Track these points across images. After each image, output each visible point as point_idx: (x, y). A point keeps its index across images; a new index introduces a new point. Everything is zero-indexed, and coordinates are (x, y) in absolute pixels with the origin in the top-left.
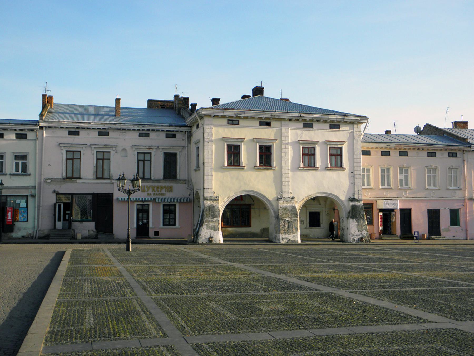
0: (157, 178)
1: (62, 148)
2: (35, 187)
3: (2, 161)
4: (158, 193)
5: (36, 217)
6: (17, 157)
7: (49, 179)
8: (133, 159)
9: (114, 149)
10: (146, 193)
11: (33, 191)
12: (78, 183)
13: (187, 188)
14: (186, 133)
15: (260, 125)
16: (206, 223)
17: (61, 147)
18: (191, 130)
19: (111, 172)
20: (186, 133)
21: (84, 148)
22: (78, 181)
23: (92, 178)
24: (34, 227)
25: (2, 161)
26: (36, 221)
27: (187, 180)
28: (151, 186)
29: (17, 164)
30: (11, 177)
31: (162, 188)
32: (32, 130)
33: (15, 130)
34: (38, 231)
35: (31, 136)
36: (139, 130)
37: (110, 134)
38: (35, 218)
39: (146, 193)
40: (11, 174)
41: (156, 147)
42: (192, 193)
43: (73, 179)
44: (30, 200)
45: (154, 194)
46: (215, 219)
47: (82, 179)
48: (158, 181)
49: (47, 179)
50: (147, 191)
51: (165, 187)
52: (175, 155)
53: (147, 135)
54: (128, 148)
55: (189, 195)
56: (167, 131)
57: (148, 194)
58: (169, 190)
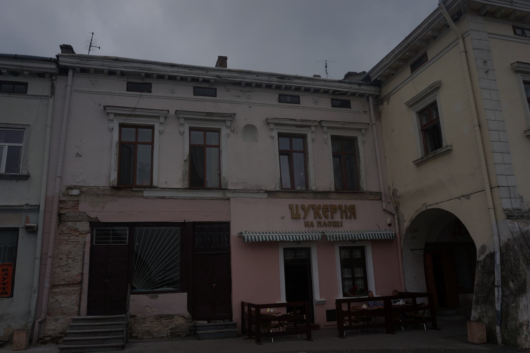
0: (321, 189)
1: (111, 117)
4: (327, 221)
5: (36, 285)
7: (75, 187)
9: (228, 123)
10: (302, 222)
11: (32, 217)
12: (147, 198)
13: (384, 210)
14: (371, 99)
17: (108, 114)
18: (380, 92)
19: (224, 174)
20: (371, 99)
21: (162, 120)
24: (29, 313)
27: (383, 193)
28: (313, 207)
31: (334, 209)
34: (37, 324)
36: (278, 87)
39: (302, 222)
41: (316, 124)
42: (396, 221)
43: (134, 189)
45: (319, 224)
47: (156, 187)
48: (325, 194)
49: (70, 188)
50: (304, 218)
51: (340, 207)
52: (353, 141)
53: (296, 100)
54: (259, 123)
55: (390, 225)
56: (334, 92)
57: (307, 225)
58: (349, 214)
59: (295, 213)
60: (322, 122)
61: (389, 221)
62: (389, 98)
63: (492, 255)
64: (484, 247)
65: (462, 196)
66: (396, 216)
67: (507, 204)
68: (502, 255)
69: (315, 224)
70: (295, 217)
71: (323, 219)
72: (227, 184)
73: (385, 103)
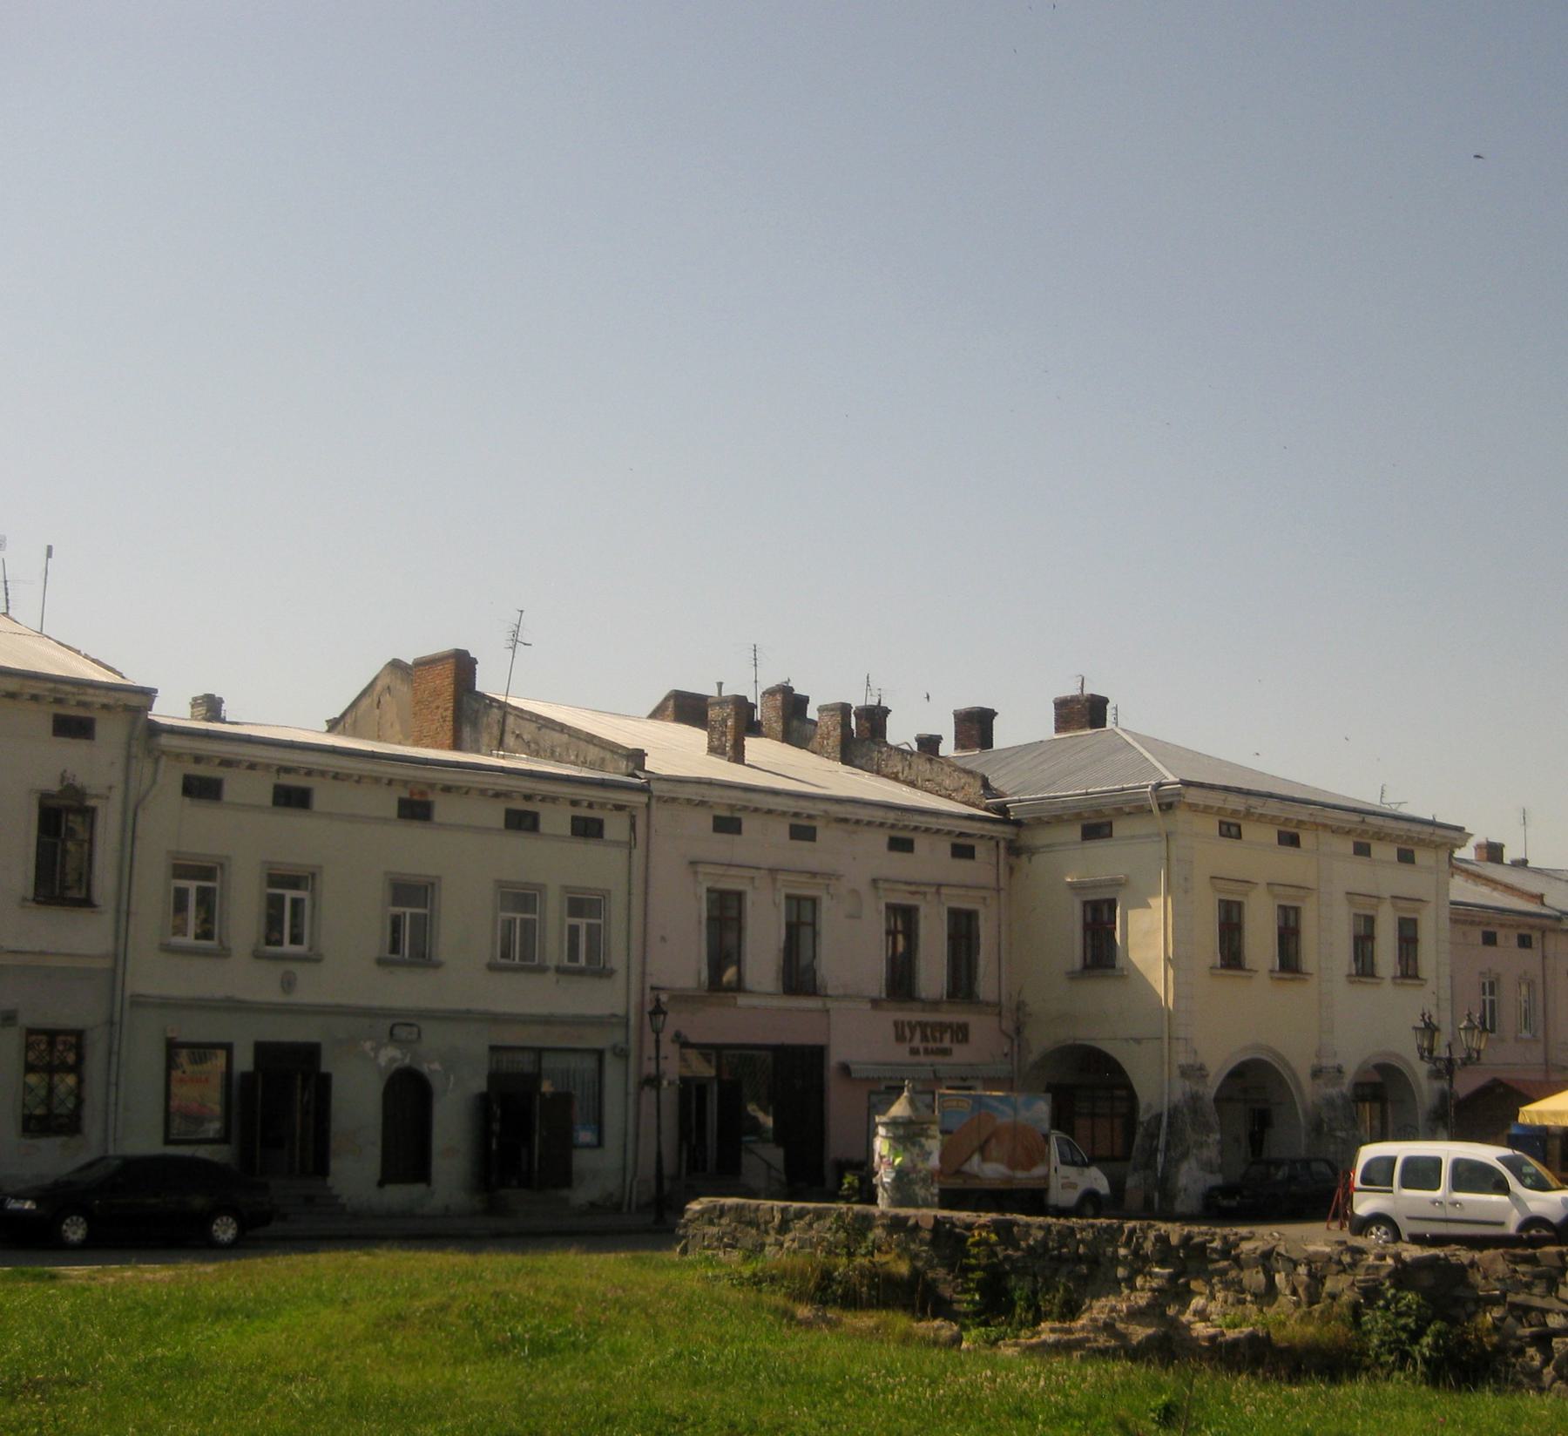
2: (627, 1018)
3: (533, 916)
6: (578, 905)
8: (874, 924)
14: (1002, 845)
15: (1355, 853)
16: (1195, 1151)
18: (1017, 835)
22: (742, 1000)
24: (624, 1168)
25: (533, 916)
26: (630, 1146)
28: (920, 1023)
29: (574, 930)
30: (558, 981)
31: (942, 1027)
32: (619, 808)
33: (574, 803)
34: (635, 1183)
35: (615, 827)
37: (744, 827)
38: (626, 1135)
40: (560, 970)
42: (1016, 1049)
46: (1211, 1135)
47: (751, 992)
48: (935, 1005)
52: (971, 916)
55: (1006, 1055)
59: (900, 1032)
61: (1006, 1050)
62: (1033, 854)
63: (1159, 1117)
64: (1150, 1106)
65: (1132, 1039)
66: (1016, 1043)
67: (1183, 1059)
68: (1169, 1117)
69: (922, 1050)
70: (900, 1038)
72: (826, 988)
73: (1024, 858)
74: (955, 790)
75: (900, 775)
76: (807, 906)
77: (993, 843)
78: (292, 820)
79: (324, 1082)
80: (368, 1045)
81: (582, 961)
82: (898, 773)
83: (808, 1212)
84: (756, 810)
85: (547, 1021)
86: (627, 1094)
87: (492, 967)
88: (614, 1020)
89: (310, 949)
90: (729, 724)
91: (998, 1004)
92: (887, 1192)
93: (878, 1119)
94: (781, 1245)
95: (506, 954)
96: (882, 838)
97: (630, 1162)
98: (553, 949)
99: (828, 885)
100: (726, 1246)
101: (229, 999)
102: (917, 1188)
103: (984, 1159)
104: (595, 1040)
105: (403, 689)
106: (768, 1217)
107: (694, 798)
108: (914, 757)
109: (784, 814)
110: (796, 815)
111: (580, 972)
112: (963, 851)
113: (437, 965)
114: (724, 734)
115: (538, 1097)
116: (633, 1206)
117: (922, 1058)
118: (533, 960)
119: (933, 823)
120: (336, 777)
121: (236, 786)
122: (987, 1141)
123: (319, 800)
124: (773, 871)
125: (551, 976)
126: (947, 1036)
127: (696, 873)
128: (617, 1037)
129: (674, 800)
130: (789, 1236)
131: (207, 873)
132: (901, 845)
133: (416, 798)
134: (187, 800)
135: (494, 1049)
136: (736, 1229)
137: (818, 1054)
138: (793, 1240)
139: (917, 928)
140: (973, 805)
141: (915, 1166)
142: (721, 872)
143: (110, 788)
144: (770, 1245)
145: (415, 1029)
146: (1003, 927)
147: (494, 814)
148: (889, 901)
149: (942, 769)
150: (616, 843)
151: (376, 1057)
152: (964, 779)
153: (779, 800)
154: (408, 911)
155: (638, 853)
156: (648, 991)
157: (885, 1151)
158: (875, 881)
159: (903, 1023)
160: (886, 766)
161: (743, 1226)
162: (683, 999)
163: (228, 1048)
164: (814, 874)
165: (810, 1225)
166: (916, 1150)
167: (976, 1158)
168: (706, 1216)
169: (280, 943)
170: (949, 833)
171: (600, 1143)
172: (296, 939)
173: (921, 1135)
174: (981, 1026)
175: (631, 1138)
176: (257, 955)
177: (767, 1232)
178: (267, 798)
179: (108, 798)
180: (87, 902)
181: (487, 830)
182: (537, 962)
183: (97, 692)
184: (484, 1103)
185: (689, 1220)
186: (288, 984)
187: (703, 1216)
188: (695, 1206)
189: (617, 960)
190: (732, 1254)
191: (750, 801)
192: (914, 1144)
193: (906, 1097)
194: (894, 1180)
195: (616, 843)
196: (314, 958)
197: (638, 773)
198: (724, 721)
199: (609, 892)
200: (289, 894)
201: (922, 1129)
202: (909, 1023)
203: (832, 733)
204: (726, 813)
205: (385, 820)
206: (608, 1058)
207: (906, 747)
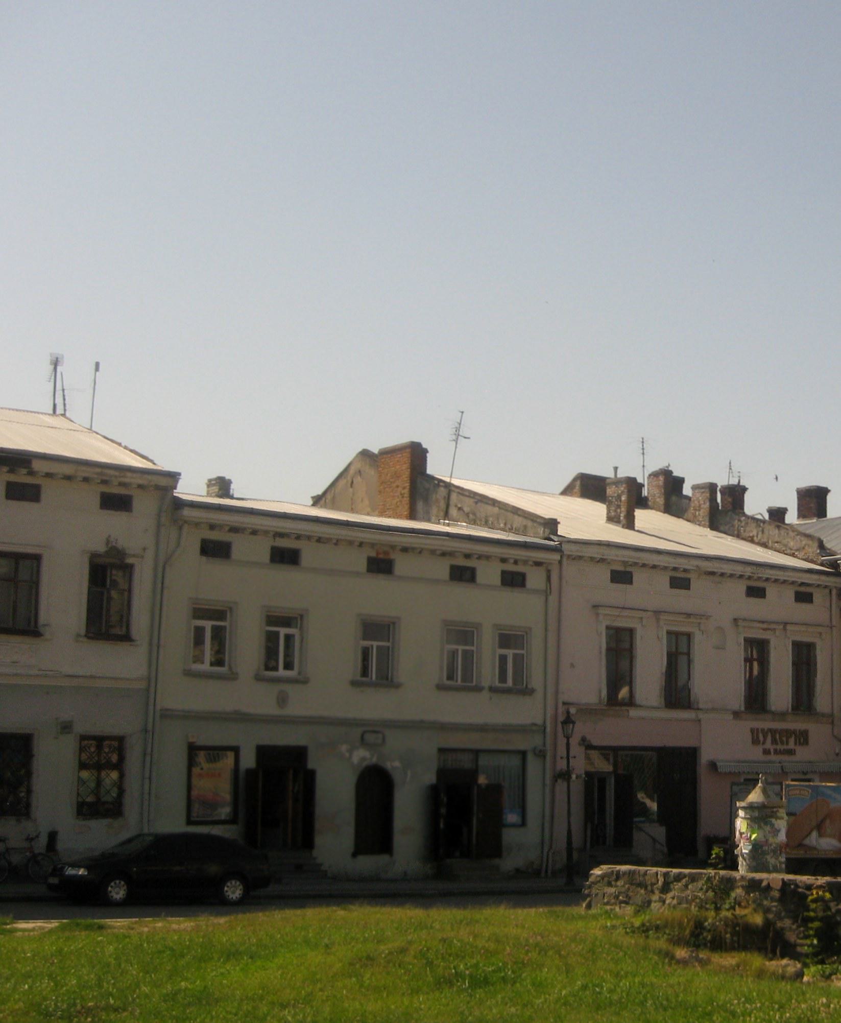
3: (472, 648)
6: (507, 639)
8: (736, 653)
13: (835, 737)
22: (633, 713)
23: (655, 704)
25: (472, 648)
26: (547, 825)
28: (770, 730)
29: (503, 659)
30: (491, 698)
31: (788, 733)
32: (538, 564)
33: (504, 560)
34: (550, 854)
35: (535, 579)
37: (635, 578)
38: (543, 817)
40: (492, 690)
44: (533, 766)
47: (640, 706)
48: (782, 716)
60: (788, 625)
69: (772, 751)
70: (755, 741)
71: (779, 747)
72: (698, 703)
74: (797, 550)
75: (755, 538)
76: (685, 638)
77: (827, 591)
78: (284, 575)
79: (311, 776)
80: (344, 748)
81: (510, 683)
82: (753, 537)
83: (685, 876)
84: (644, 565)
85: (483, 729)
86: (544, 785)
87: (440, 687)
88: (534, 728)
89: (299, 673)
90: (623, 498)
91: (832, 715)
92: (745, 860)
93: (738, 804)
94: (664, 902)
95: (450, 677)
96: (742, 587)
97: (547, 836)
98: (487, 673)
99: (699, 623)
100: (621, 902)
101: (237, 712)
102: (768, 857)
103: (821, 835)
104: (520, 743)
105: (371, 473)
106: (654, 880)
107: (596, 556)
108: (766, 525)
109: (665, 568)
110: (675, 569)
111: (508, 691)
112: (804, 597)
113: (398, 686)
114: (619, 507)
115: (476, 787)
116: (549, 872)
117: (773, 757)
118: (472, 682)
119: (781, 575)
120: (319, 540)
121: (241, 547)
122: (823, 821)
123: (307, 558)
124: (657, 613)
125: (485, 694)
126: (792, 741)
127: (597, 615)
128: (537, 741)
129: (580, 558)
130: (670, 895)
131: (220, 615)
132: (756, 592)
133: (381, 556)
134: (204, 558)
135: (442, 750)
136: (629, 889)
137: (690, 755)
138: (673, 898)
139: (768, 656)
140: (812, 561)
141: (767, 841)
142: (617, 614)
143: (144, 549)
144: (655, 902)
145: (380, 736)
146: (835, 656)
147: (442, 569)
148: (746, 636)
149: (787, 534)
150: (535, 591)
151: (350, 757)
152: (805, 541)
153: (661, 557)
154: (375, 644)
155: (553, 598)
156: (560, 705)
157: (744, 830)
158: (735, 620)
159: (758, 729)
160: (745, 531)
161: (635, 887)
162: (588, 711)
163: (236, 750)
164: (689, 615)
165: (686, 886)
166: (768, 828)
167: (814, 834)
168: (606, 879)
169: (276, 669)
170: (793, 583)
171: (523, 824)
172: (288, 666)
173: (772, 817)
174: (818, 732)
175: (547, 818)
176: (258, 678)
177: (653, 892)
178: (266, 557)
179: (142, 557)
180: (126, 638)
181: (437, 581)
182: (474, 684)
183: (135, 475)
184: (434, 792)
185: (593, 883)
186: (282, 700)
187: (603, 879)
188: (597, 872)
189: (536, 682)
190: (626, 909)
191: (639, 558)
192: (766, 824)
193: (760, 787)
194: (751, 851)
195: (535, 591)
196: (302, 681)
197: (552, 537)
198: (619, 497)
199: (530, 629)
200: (283, 631)
201: (773, 812)
202: (763, 730)
203: (702, 506)
204: (620, 568)
205: (357, 574)
206: (530, 757)
207: (759, 517)
